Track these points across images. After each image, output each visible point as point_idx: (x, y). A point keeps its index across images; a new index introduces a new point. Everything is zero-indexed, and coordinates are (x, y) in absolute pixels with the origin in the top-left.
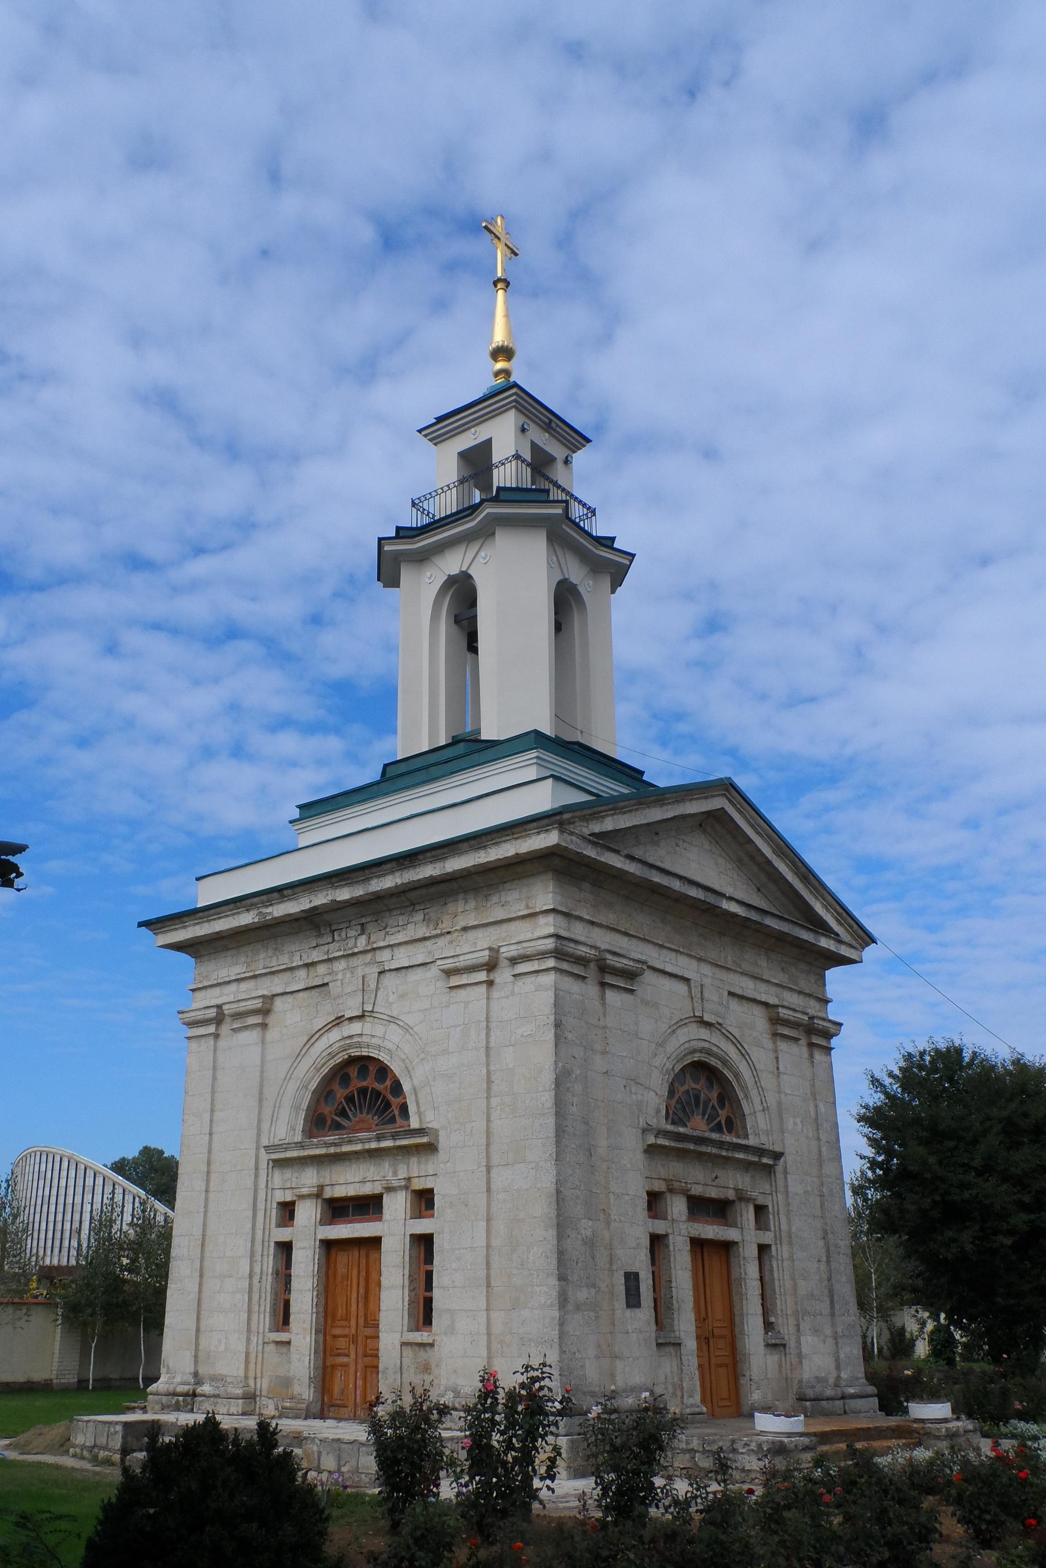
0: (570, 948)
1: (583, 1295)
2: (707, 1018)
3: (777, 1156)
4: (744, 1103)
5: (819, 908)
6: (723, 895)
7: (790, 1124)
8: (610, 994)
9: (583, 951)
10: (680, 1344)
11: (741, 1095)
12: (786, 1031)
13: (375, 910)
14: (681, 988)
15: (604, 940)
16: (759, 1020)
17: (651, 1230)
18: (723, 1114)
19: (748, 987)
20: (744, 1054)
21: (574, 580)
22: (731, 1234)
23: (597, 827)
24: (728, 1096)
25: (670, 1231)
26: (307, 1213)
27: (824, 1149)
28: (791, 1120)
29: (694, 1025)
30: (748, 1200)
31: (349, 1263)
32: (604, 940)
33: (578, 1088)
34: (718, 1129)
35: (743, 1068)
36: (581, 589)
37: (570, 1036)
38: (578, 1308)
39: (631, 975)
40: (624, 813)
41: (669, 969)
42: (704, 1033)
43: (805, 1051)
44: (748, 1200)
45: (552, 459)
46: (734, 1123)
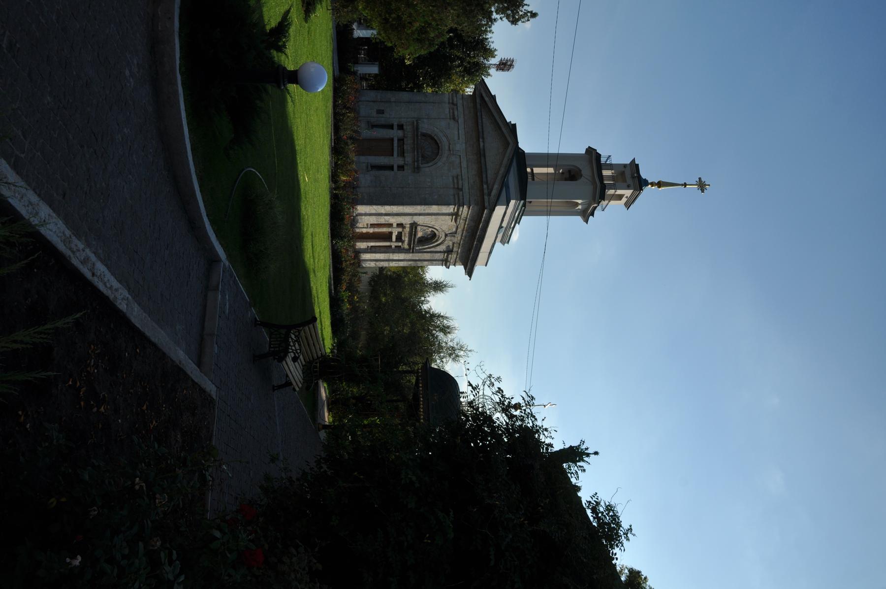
5: (496, 186)
6: (483, 138)
14: (456, 138)
15: (460, 108)
19: (464, 165)
23: (484, 95)
31: (385, 147)
32: (460, 108)
35: (440, 164)
42: (447, 148)
45: (625, 181)
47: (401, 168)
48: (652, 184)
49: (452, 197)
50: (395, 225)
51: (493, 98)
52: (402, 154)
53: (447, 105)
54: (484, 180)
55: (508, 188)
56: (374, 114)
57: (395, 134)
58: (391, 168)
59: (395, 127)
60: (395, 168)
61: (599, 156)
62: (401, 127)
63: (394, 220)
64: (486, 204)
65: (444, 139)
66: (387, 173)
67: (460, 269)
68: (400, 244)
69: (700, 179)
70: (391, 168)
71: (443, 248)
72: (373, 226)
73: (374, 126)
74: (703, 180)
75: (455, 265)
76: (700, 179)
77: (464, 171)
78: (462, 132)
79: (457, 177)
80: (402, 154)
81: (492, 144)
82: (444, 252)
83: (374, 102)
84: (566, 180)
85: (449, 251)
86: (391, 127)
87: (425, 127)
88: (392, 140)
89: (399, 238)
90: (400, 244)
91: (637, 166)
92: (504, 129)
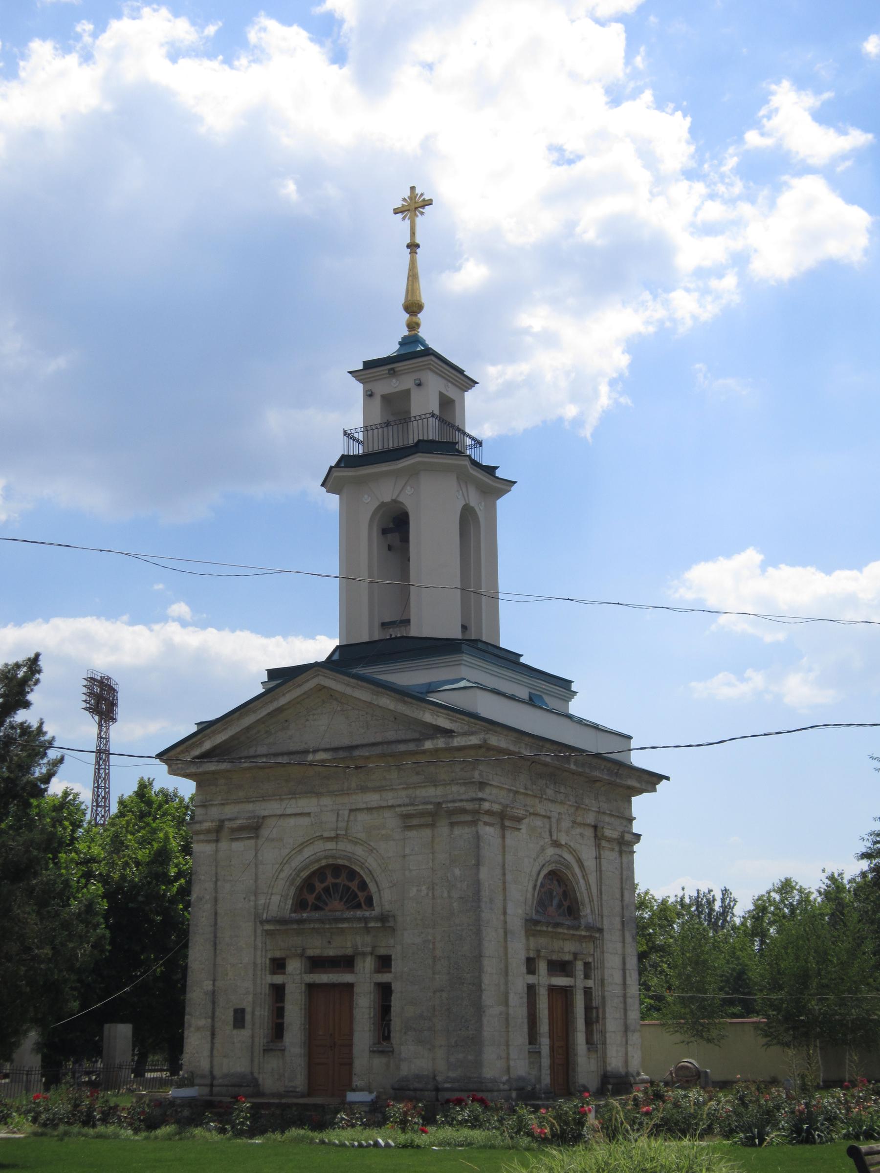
1: (202, 1022)
2: (326, 834)
5: (428, 717)
7: (413, 891)
10: (284, 1050)
12: (415, 822)
14: (305, 821)
15: (229, 811)
16: (391, 821)
17: (270, 982)
20: (372, 850)
21: (387, 499)
22: (347, 978)
23: (197, 752)
25: (286, 981)
27: (455, 904)
28: (415, 889)
29: (321, 842)
30: (364, 954)
31: (329, 1003)
33: (208, 906)
34: (358, 906)
35: (372, 863)
36: (400, 499)
37: (203, 878)
38: (198, 1029)
40: (220, 732)
41: (289, 811)
42: (330, 845)
44: (364, 954)
45: (407, 393)
46: (369, 901)
48: (413, 326)
49: (457, 831)
50: (531, 979)
51: (205, 728)
52: (347, 962)
53: (224, 845)
54: (412, 747)
55: (432, 688)
56: (244, 1034)
57: (295, 976)
58: (385, 990)
60: (385, 978)
61: (346, 461)
62: (278, 965)
63: (519, 981)
64: (474, 740)
65: (307, 852)
66: (396, 1002)
67: (640, 804)
68: (579, 965)
69: (396, 211)
71: (588, 854)
72: (533, 1037)
73: (278, 1030)
74: (399, 204)
75: (631, 820)
76: (396, 211)
77: (390, 798)
79: (406, 817)
80: (347, 962)
81: (325, 729)
82: (598, 846)
83: (213, 1035)
84: (405, 539)
85: (598, 835)
86: (278, 992)
87: (278, 900)
88: (311, 988)
89: (561, 967)
90: (579, 965)
91: (368, 365)
92: (282, 701)
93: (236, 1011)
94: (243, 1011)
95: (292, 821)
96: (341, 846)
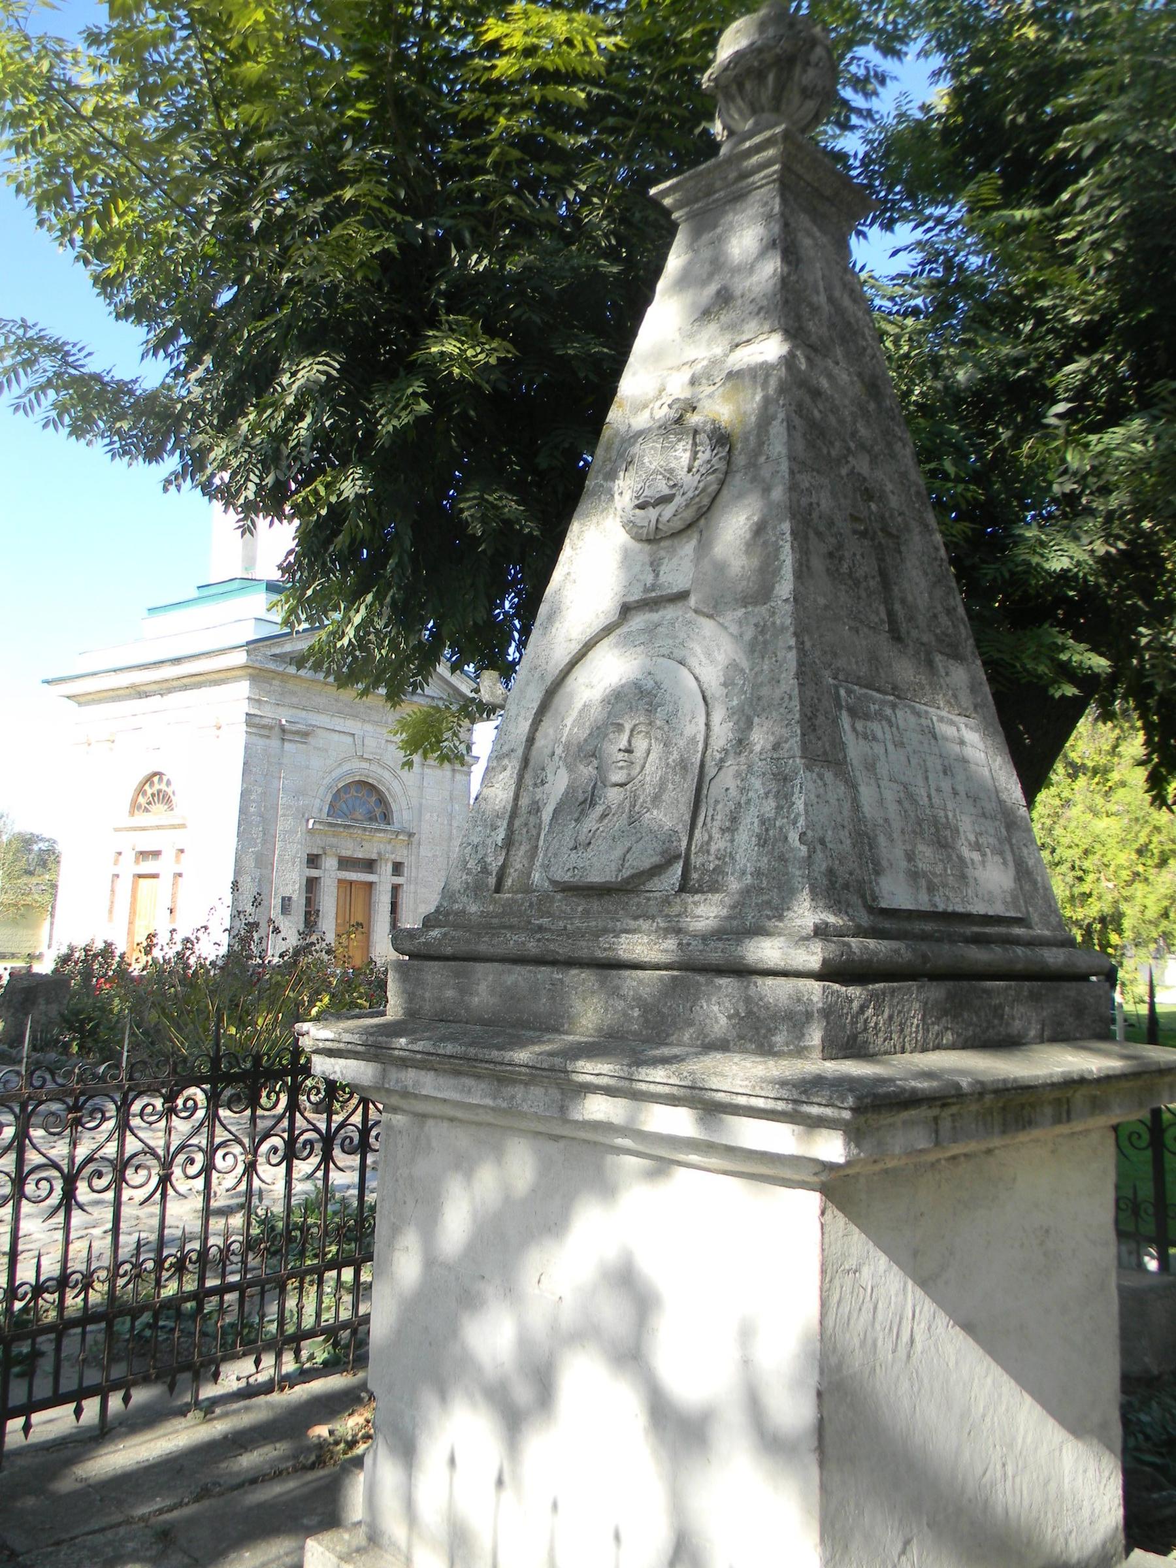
0: (257, 720)
3: (411, 835)
4: (393, 806)
7: (427, 816)
8: (287, 745)
9: (265, 721)
11: (391, 800)
13: (166, 688)
14: (349, 740)
18: (378, 812)
23: (277, 651)
24: (382, 801)
26: (129, 856)
35: (396, 787)
39: (306, 734)
42: (365, 765)
43: (449, 774)
46: (386, 817)
47: (397, 868)
52: (369, 865)
59: (314, 873)
65: (346, 767)
70: (396, 889)
78: (339, 723)
88: (340, 881)
93: (283, 899)
94: (290, 899)
95: (336, 736)
96: (373, 768)
